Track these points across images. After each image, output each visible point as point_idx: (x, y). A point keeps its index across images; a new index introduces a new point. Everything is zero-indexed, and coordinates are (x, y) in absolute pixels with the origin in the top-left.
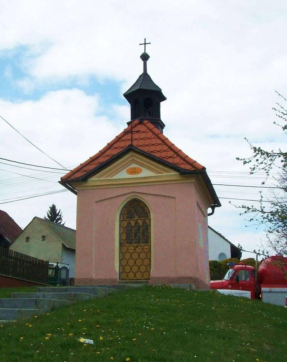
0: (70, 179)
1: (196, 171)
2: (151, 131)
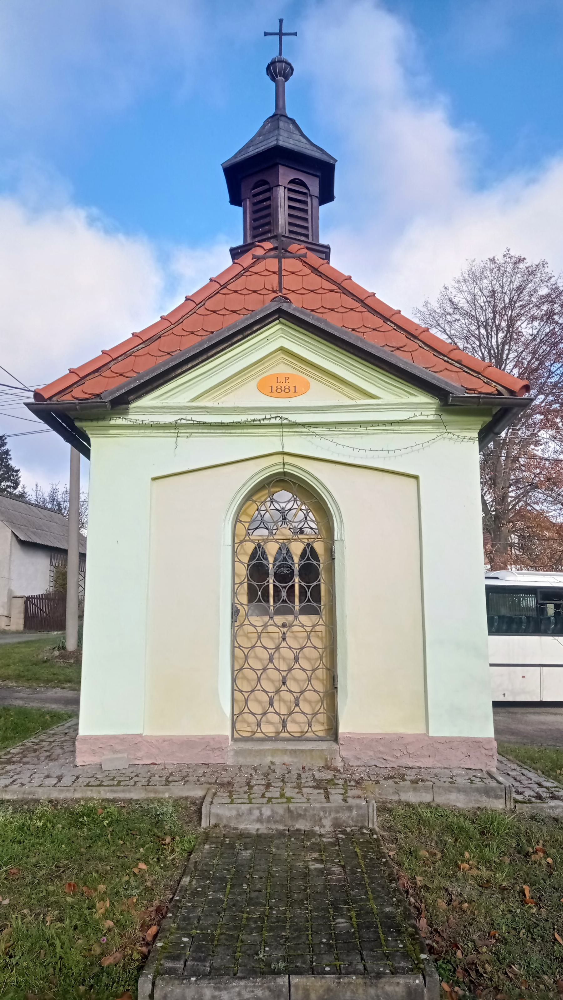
0: (68, 397)
1: (500, 393)
2: (315, 270)
